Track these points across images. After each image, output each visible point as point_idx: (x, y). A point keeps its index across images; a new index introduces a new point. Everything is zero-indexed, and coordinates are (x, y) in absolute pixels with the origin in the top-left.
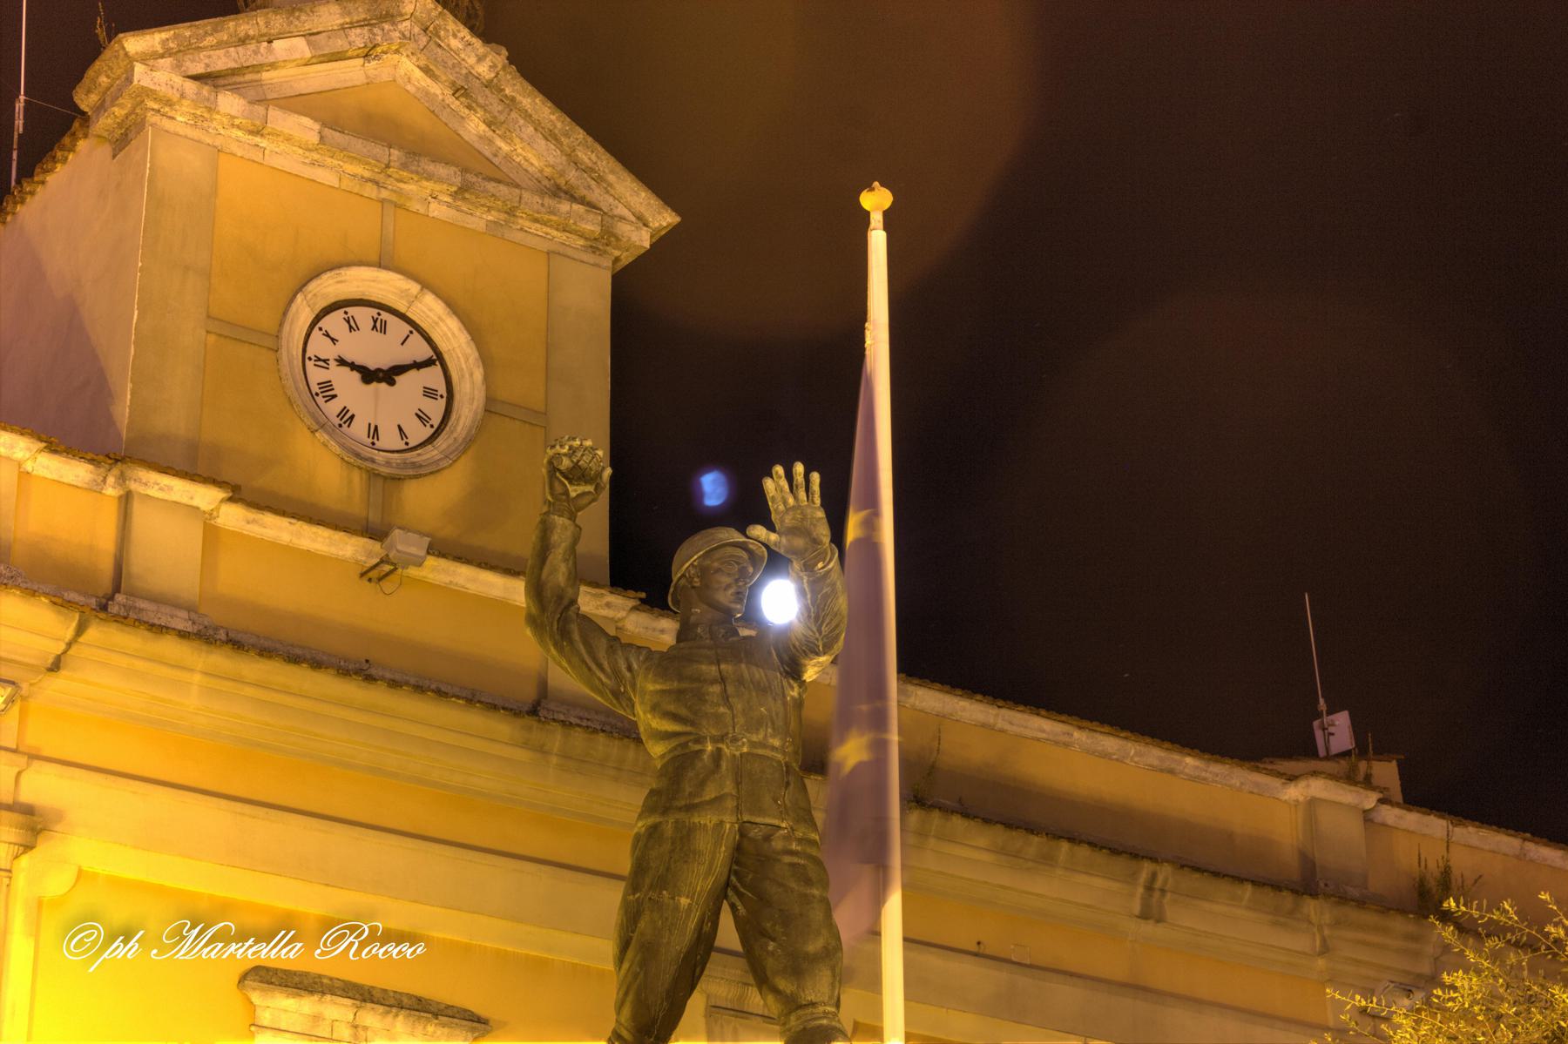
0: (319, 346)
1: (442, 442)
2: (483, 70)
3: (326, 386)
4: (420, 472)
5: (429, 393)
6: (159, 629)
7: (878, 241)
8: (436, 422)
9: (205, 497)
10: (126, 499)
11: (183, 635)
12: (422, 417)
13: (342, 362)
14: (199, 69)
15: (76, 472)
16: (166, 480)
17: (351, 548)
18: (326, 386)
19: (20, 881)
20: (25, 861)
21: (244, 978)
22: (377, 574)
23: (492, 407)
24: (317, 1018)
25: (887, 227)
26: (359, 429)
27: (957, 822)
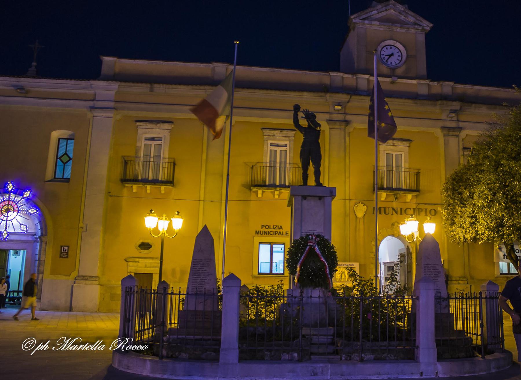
0: (382, 52)
1: (401, 63)
2: (402, 9)
3: (384, 58)
4: (398, 68)
5: (399, 56)
6: (361, 95)
9: (367, 76)
10: (357, 78)
11: (364, 95)
12: (398, 60)
14: (362, 18)
15: (350, 76)
19: (347, 130)
22: (392, 82)
23: (408, 56)
27: (481, 105)
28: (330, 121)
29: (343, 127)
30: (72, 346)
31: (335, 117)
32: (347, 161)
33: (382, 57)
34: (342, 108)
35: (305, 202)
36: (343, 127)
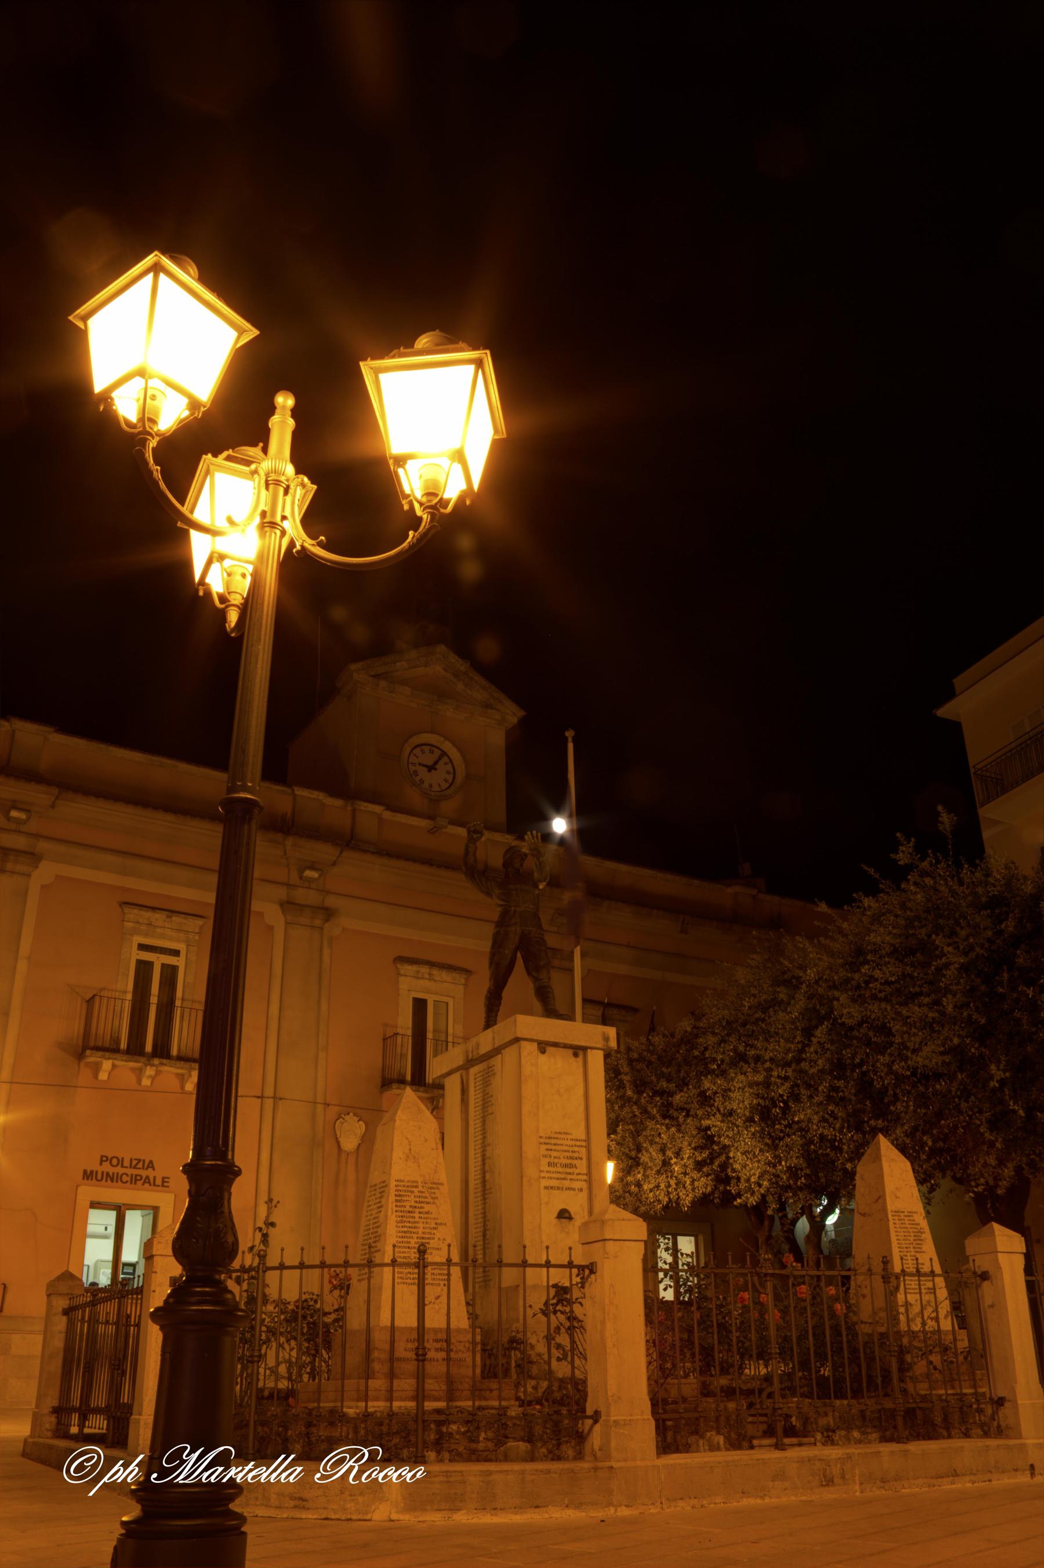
0: (412, 759)
2: (462, 668)
3: (415, 772)
6: (365, 851)
7: (571, 746)
8: (450, 781)
9: (378, 809)
10: (354, 811)
11: (373, 853)
12: (446, 781)
13: (420, 764)
14: (373, 673)
15: (339, 803)
16: (366, 804)
17: (424, 823)
18: (415, 772)
20: (327, 925)
21: (395, 960)
22: (432, 831)
24: (418, 972)
25: (573, 742)
26: (426, 785)
28: (288, 905)
29: (318, 922)
30: (206, 1469)
31: (302, 895)
32: (324, 1007)
33: (412, 768)
34: (320, 876)
35: (543, 1059)
36: (318, 922)
